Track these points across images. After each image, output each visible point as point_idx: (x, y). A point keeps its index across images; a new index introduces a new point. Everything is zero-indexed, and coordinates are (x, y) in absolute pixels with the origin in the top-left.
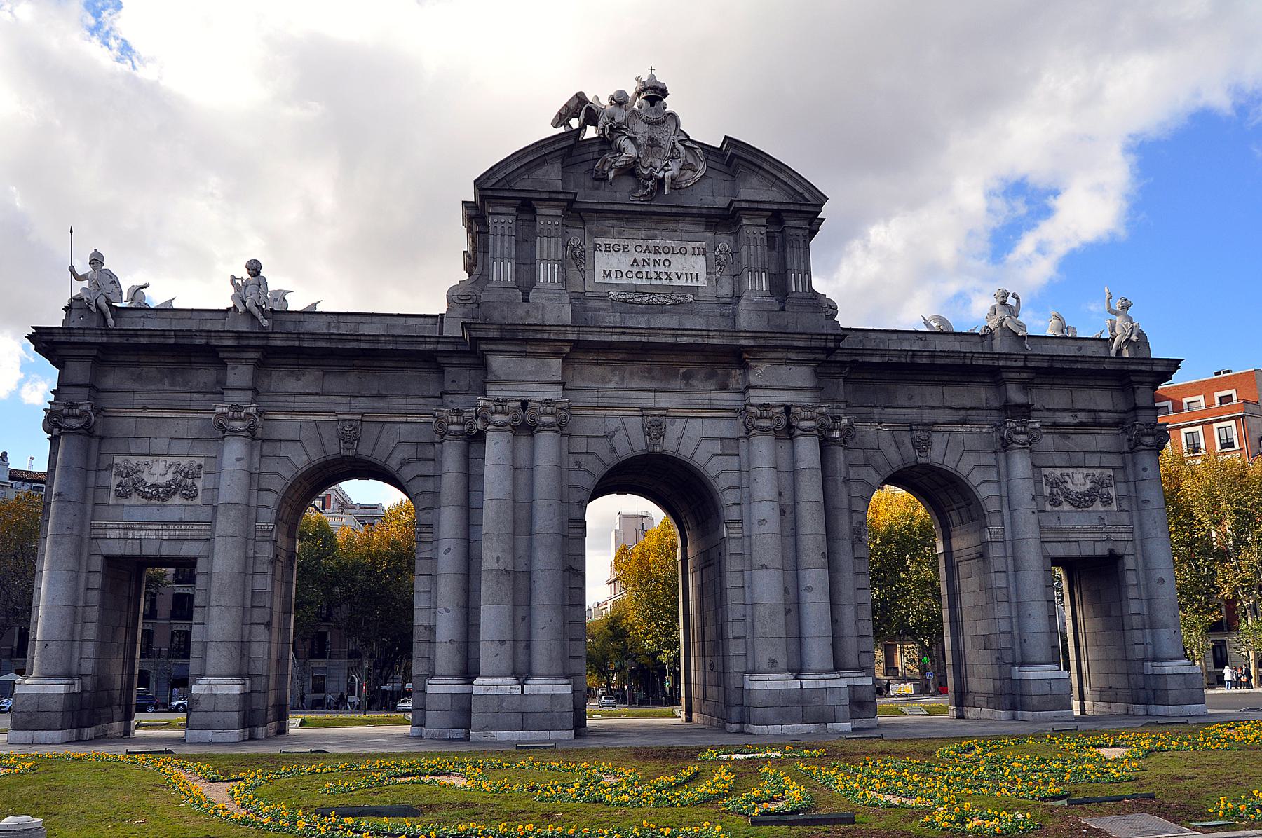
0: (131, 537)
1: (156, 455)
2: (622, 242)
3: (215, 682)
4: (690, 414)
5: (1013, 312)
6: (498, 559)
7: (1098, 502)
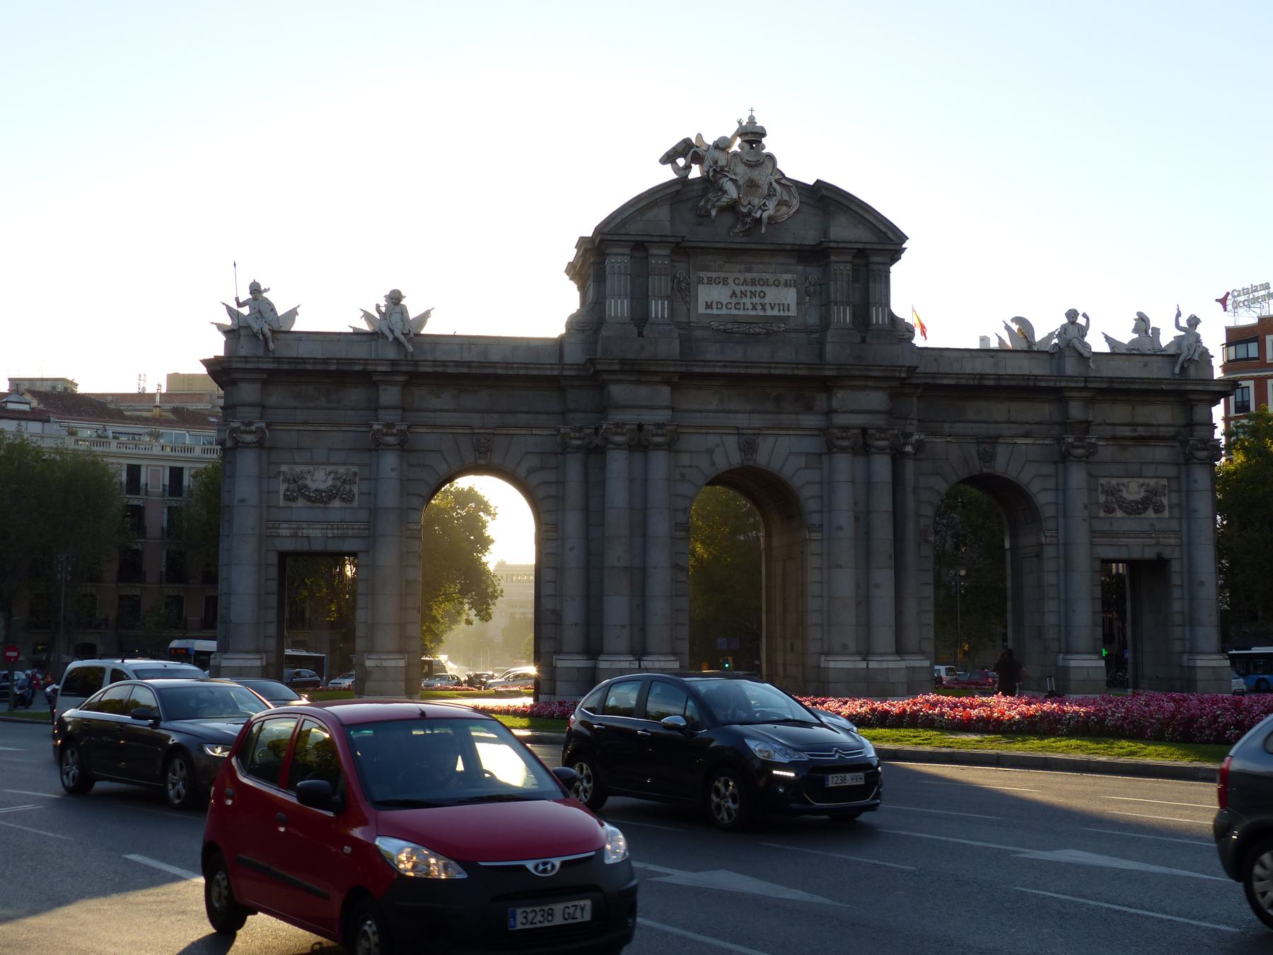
0: (300, 535)
2: (722, 275)
3: (385, 657)
5: (1083, 331)
6: (619, 558)
7: (1151, 507)
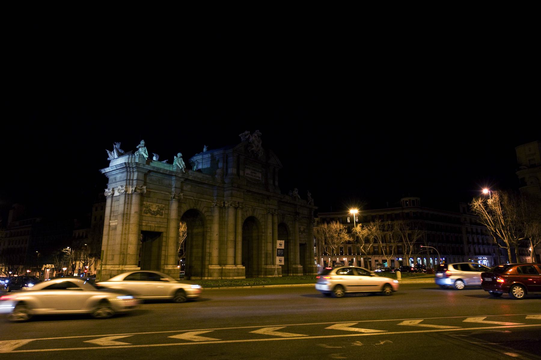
1: (154, 203)
4: (259, 208)
